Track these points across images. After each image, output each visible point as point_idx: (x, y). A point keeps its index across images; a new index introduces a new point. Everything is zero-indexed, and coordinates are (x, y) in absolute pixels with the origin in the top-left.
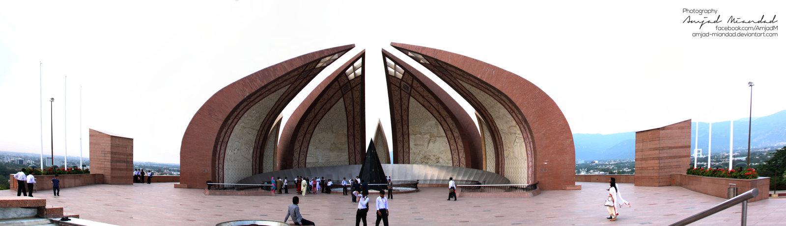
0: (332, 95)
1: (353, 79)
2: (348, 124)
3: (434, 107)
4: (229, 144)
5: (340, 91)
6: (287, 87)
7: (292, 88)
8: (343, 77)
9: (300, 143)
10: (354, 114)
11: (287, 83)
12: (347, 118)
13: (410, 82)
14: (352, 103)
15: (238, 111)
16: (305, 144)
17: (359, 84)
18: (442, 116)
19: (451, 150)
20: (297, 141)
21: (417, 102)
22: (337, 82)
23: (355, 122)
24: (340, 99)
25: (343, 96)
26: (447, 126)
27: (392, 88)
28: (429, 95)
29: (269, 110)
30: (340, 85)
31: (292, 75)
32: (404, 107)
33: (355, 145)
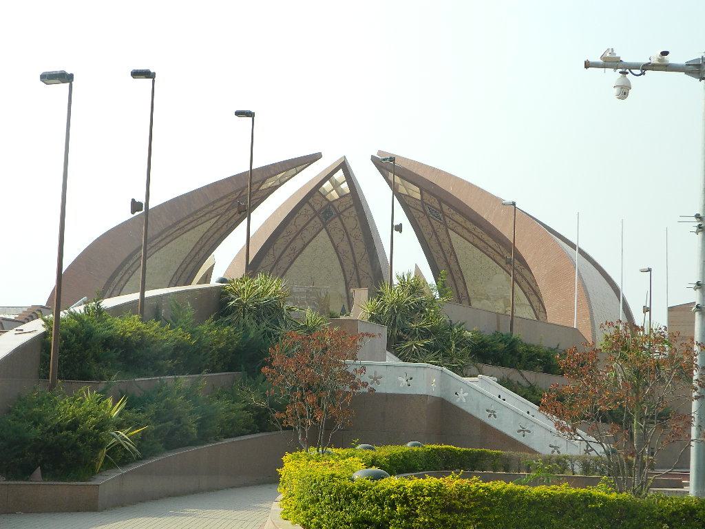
0: (302, 225)
1: (337, 200)
2: (345, 276)
3: (493, 249)
5: (317, 219)
6: (214, 220)
7: (223, 219)
8: (317, 196)
10: (354, 258)
12: (341, 264)
13: (437, 206)
15: (131, 262)
17: (351, 206)
25: (325, 226)
27: (414, 214)
29: (185, 255)
30: (314, 210)
31: (219, 204)
32: (446, 246)
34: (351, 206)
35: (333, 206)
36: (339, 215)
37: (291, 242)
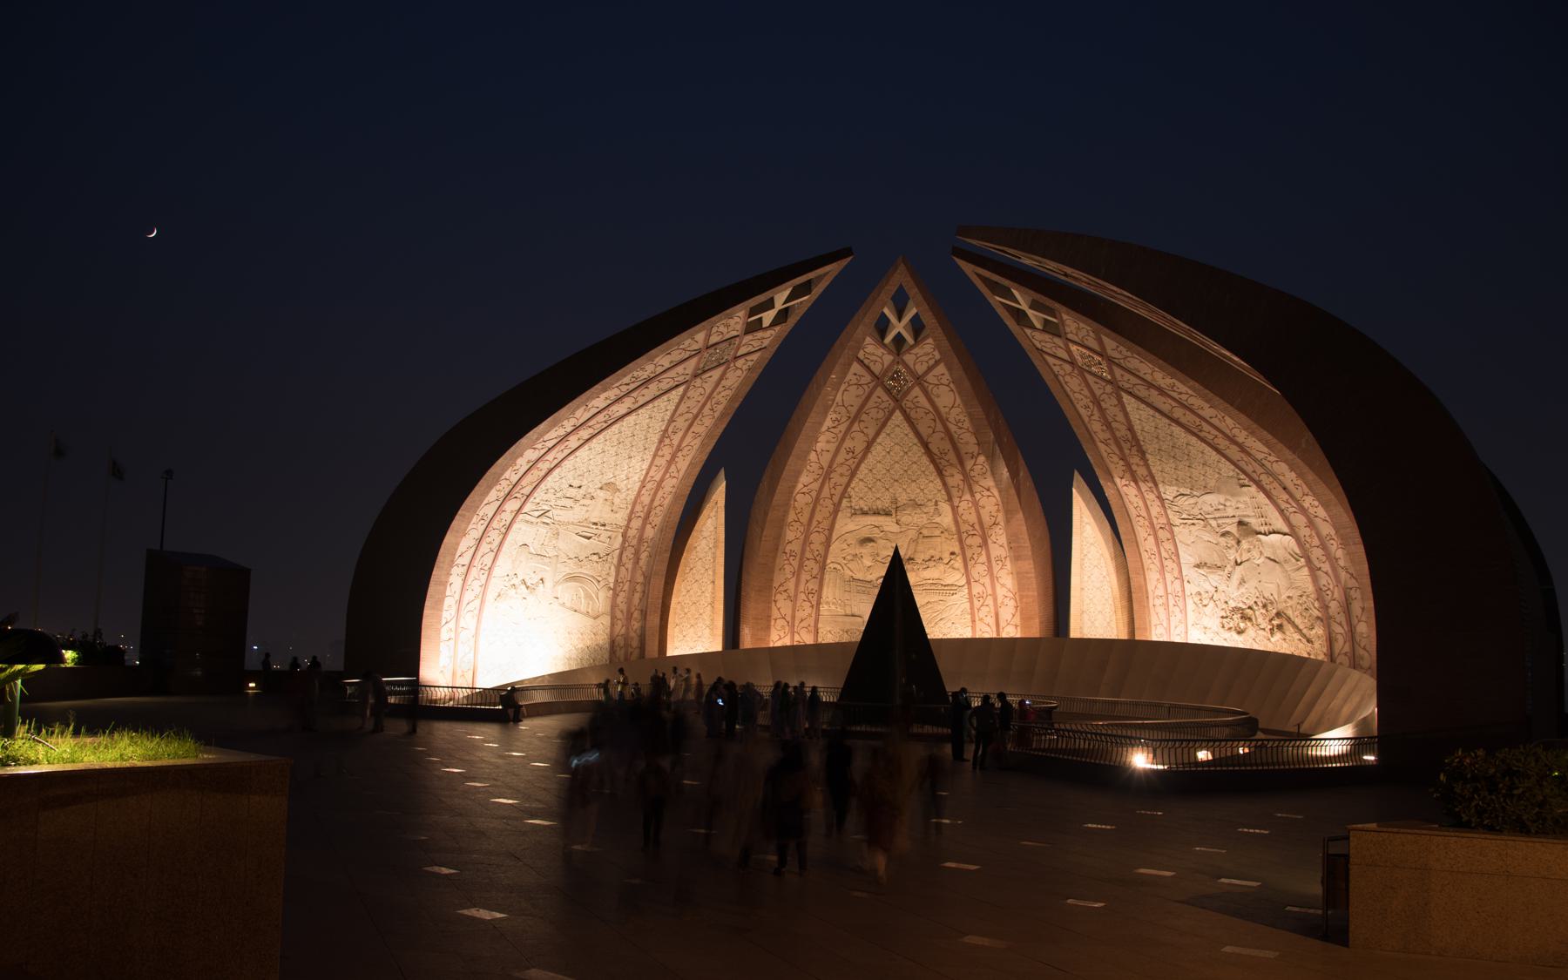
4: (497, 571)
9: (795, 563)
11: (664, 386)
14: (939, 427)
16: (811, 565)
17: (937, 363)
18: (1256, 460)
19: (1319, 590)
20: (781, 560)
21: (1152, 412)
22: (856, 367)
23: (977, 488)
24: (888, 419)
26: (1286, 497)
27: (1056, 369)
28: (1178, 384)
33: (990, 569)
34: (937, 363)
35: (906, 365)
36: (919, 380)
37: (843, 440)
